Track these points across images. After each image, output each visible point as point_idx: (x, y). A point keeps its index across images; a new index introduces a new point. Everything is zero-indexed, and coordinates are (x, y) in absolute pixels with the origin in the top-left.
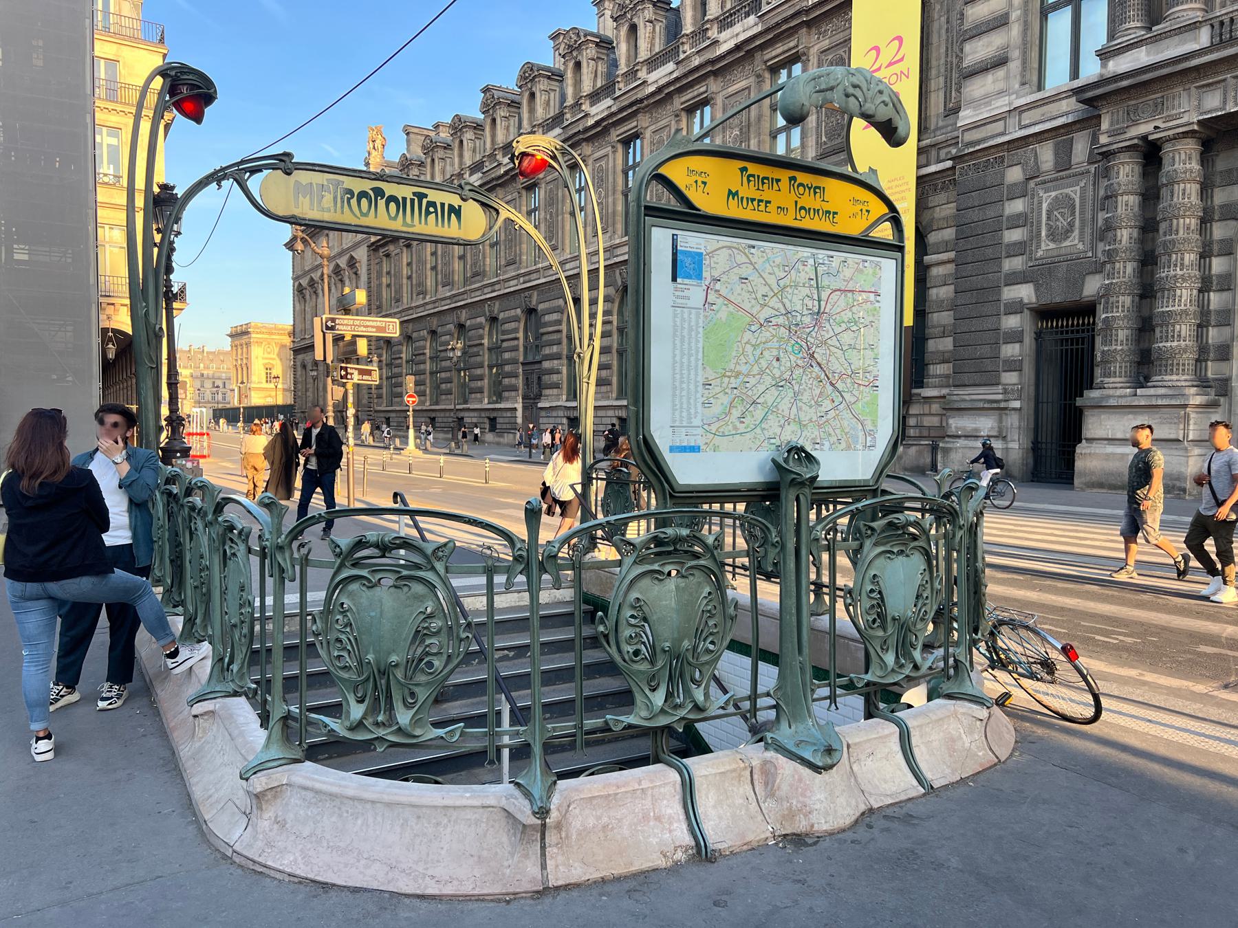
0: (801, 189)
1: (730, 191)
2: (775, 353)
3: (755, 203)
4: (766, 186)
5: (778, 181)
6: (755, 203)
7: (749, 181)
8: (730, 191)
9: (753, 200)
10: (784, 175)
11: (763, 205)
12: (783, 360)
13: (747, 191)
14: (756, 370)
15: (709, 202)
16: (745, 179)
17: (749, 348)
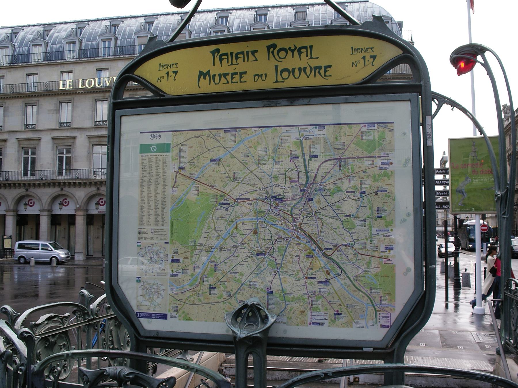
0: (282, 54)
1: (201, 74)
2: (251, 227)
3: (229, 77)
4: (240, 60)
5: (254, 52)
6: (229, 77)
7: (221, 60)
8: (201, 74)
9: (225, 75)
10: (261, 46)
11: (237, 78)
12: (262, 234)
13: (226, 68)
14: (230, 243)
15: (171, 88)
16: (217, 59)
17: (221, 223)
